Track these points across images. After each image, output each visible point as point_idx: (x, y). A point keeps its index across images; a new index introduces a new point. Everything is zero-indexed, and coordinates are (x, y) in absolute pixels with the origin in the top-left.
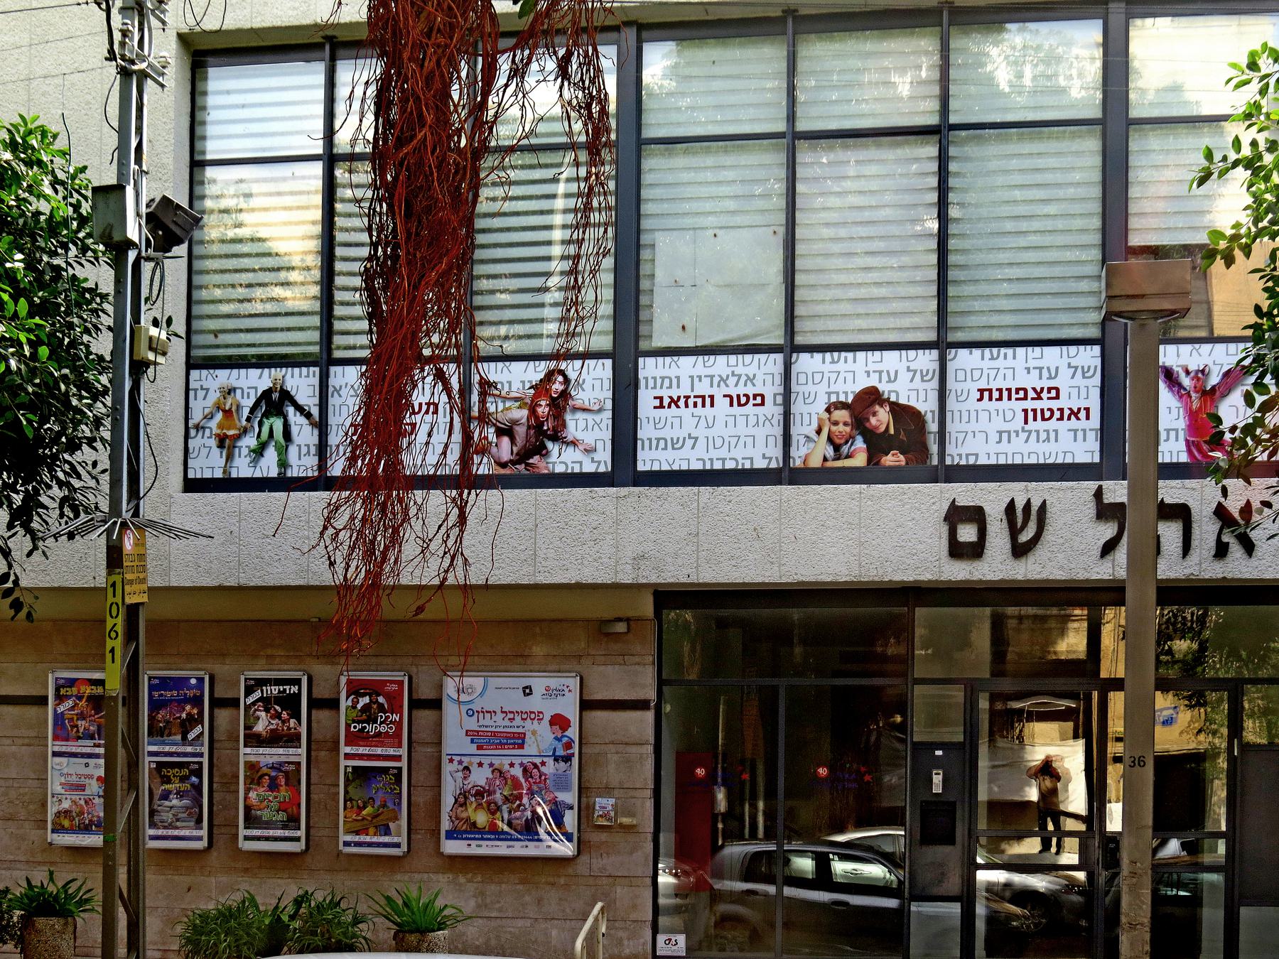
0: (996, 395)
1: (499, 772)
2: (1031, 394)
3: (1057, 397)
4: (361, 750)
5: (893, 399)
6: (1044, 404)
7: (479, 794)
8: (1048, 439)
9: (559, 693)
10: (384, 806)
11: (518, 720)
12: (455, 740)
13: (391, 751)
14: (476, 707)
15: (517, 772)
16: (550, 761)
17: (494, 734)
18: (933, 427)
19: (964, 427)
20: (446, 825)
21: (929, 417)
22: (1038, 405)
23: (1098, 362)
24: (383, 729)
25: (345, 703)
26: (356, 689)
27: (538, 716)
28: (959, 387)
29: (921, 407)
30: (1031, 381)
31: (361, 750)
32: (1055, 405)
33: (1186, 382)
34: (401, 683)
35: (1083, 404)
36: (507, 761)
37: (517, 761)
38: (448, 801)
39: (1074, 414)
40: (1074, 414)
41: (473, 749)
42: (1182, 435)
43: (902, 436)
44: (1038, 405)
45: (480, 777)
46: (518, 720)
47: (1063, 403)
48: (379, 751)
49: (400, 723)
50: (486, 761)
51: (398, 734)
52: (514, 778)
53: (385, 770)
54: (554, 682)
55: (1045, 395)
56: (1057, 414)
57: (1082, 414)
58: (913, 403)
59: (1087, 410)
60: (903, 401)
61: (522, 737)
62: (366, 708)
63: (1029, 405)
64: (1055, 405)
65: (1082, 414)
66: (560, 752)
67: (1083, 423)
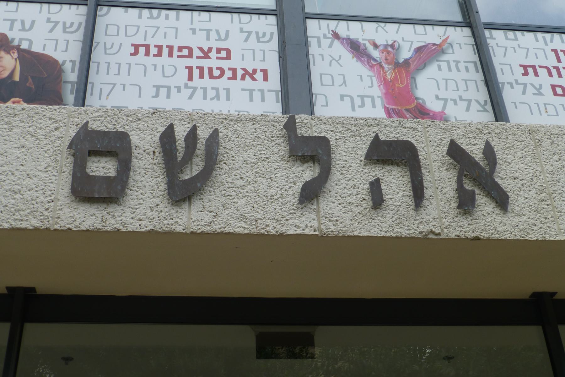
0: (153, 50)
2: (196, 52)
3: (228, 57)
5: (25, 46)
6: (213, 63)
8: (217, 97)
18: (71, 76)
19: (111, 78)
21: (68, 67)
22: (205, 63)
23: (275, 29)
28: (109, 41)
29: (59, 56)
30: (197, 41)
32: (225, 64)
33: (376, 54)
35: (259, 66)
39: (250, 74)
40: (250, 74)
42: (378, 102)
43: (30, 83)
44: (205, 63)
47: (236, 62)
55: (213, 54)
56: (229, 74)
57: (259, 76)
58: (49, 52)
59: (265, 72)
60: (37, 48)
63: (194, 62)
64: (225, 64)
65: (259, 76)
67: (260, 84)
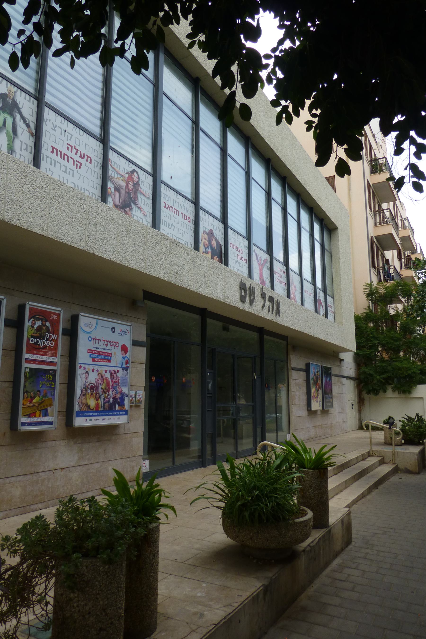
1: (100, 375)
4: (35, 357)
7: (92, 388)
9: (123, 333)
10: (45, 396)
11: (109, 347)
12: (83, 356)
13: (51, 359)
14: (93, 337)
15: (108, 375)
16: (120, 369)
17: (99, 353)
20: (77, 408)
24: (48, 344)
25: (28, 323)
26: (36, 314)
27: (115, 344)
31: (35, 357)
34: (59, 315)
36: (104, 369)
37: (108, 369)
38: (78, 392)
41: (90, 361)
45: (93, 378)
46: (109, 347)
48: (45, 358)
49: (56, 341)
50: (96, 368)
51: (55, 349)
52: (107, 379)
53: (46, 371)
54: (124, 328)
61: (110, 355)
62: (39, 329)
66: (124, 366)
